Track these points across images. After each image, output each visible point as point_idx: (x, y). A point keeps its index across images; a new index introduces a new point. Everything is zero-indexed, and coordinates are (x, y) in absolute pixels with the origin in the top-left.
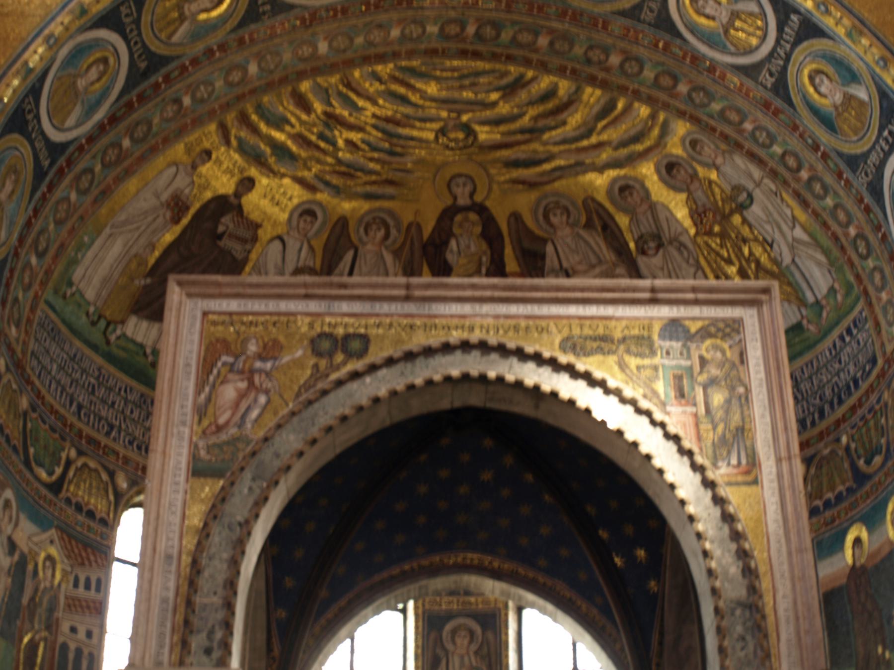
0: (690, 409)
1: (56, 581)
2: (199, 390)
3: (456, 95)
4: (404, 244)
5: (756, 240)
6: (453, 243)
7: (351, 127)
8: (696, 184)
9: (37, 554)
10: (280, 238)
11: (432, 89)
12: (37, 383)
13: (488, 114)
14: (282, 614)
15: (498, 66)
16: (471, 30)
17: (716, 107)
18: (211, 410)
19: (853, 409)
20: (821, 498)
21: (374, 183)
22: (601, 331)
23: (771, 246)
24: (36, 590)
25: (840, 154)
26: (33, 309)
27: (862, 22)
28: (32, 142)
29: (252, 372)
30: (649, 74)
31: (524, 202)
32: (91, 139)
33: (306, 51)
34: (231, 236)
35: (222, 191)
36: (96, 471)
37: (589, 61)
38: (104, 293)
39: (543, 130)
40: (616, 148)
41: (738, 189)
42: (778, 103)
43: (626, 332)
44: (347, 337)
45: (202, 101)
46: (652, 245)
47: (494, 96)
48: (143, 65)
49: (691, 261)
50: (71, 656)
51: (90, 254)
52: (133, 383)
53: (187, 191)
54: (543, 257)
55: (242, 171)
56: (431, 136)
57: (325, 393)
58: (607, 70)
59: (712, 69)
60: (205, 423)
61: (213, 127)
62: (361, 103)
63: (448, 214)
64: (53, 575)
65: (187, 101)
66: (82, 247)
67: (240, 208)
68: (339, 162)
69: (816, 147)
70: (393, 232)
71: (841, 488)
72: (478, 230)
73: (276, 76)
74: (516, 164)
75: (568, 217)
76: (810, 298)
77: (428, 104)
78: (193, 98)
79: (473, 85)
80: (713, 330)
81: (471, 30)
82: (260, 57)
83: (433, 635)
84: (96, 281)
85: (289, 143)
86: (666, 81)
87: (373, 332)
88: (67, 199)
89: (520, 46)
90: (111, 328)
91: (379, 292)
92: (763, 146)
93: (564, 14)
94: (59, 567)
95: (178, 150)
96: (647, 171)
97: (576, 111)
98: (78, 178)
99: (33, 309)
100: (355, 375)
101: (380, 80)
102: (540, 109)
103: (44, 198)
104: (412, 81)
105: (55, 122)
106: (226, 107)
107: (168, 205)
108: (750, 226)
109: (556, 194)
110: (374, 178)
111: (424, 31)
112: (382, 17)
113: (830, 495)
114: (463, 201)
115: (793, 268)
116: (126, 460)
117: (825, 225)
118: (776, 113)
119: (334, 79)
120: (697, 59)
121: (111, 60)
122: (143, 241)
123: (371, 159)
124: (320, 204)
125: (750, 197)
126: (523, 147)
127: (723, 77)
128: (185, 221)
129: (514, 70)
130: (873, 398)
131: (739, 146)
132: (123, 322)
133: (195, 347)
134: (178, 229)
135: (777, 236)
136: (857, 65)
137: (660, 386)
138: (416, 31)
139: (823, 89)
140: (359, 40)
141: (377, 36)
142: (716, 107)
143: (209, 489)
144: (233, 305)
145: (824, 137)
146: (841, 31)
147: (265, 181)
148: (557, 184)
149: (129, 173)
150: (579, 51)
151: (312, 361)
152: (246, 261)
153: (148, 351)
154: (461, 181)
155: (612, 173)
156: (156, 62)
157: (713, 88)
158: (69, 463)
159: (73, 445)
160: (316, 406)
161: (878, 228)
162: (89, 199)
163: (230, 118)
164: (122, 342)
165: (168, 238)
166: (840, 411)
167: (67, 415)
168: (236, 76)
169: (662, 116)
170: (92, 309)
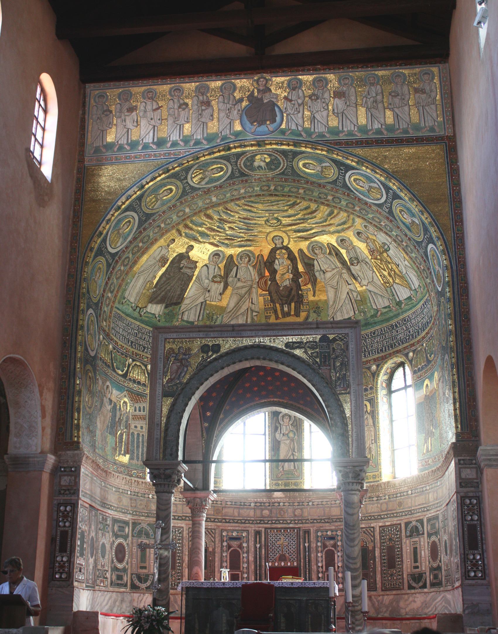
0: (328, 368)
1: (128, 411)
2: (164, 367)
3: (271, 208)
4: (256, 263)
5: (393, 263)
6: (277, 261)
7: (230, 222)
8: (368, 241)
9: (120, 402)
10: (206, 265)
11: (260, 206)
12: (115, 338)
13: (285, 214)
14: (206, 425)
15: (285, 199)
16: (272, 188)
17: (370, 216)
18: (169, 374)
19: (427, 333)
20: (417, 367)
21: (242, 241)
22: (299, 340)
23: (398, 266)
24: (121, 415)
25: (414, 240)
26: (111, 313)
27: (414, 195)
28: (105, 257)
29: (182, 359)
30: (344, 203)
31: (304, 245)
32: (127, 247)
33: (208, 201)
34: (186, 267)
35: (181, 252)
36: (140, 366)
37: (320, 198)
38: (138, 298)
39: (308, 219)
40: (337, 226)
41: (384, 244)
42: (391, 218)
43: (308, 340)
44: (213, 345)
45: (169, 224)
46: (355, 262)
47: (286, 208)
48: (144, 219)
49: (371, 269)
50: (136, 437)
51: (131, 285)
53: (166, 254)
54: (313, 266)
55: (188, 243)
56: (264, 223)
57: (205, 366)
58: (328, 201)
59: (366, 203)
60: (167, 378)
61: (174, 231)
62: (232, 214)
63: (273, 251)
64: (127, 408)
65: (163, 225)
66: (127, 284)
67: (189, 257)
68: (227, 235)
69: (406, 235)
70: (252, 258)
71: (423, 364)
72: (286, 256)
73: (197, 211)
74: (299, 231)
75: (322, 251)
76: (413, 288)
77: (260, 212)
78: (165, 224)
79: (278, 204)
80: (337, 338)
81: (272, 188)
82: (189, 206)
83: (275, 418)
84: (134, 295)
85: (206, 231)
86: (351, 206)
87: (221, 342)
88: (120, 270)
89: (293, 192)
90: (142, 310)
91: (224, 329)
92: (390, 231)
93: (307, 182)
94: (128, 405)
95: (162, 242)
96: (350, 235)
97: (319, 213)
98: (124, 261)
99: (111, 313)
100: (215, 359)
101: (239, 206)
102: (305, 212)
103: (111, 273)
104: (253, 205)
105: (113, 246)
106: (179, 224)
107: (159, 260)
108: (390, 258)
109: (316, 242)
110: (242, 239)
111: (254, 189)
112: (235, 187)
113: (420, 366)
114: (278, 246)
115: (406, 275)
117: (414, 262)
118: (391, 221)
119: (221, 208)
120: (359, 199)
121: (132, 220)
122: (151, 276)
123: (240, 233)
124: (221, 251)
125: (388, 246)
126: (301, 225)
127: (370, 206)
128: (167, 266)
129: (292, 200)
130: (432, 331)
131: (381, 229)
132: (146, 307)
133: (163, 351)
134: (164, 269)
135: (400, 263)
136: (414, 211)
137: (318, 360)
138: (250, 190)
139: (405, 216)
140: (228, 195)
141: (235, 193)
142: (370, 216)
143: (169, 401)
144: (175, 335)
145: (408, 233)
146: (407, 198)
147: (197, 245)
148: (316, 238)
149: (143, 254)
150: (316, 194)
152: (193, 275)
153: (157, 316)
154: (277, 238)
155: (337, 234)
156: (148, 216)
157: (368, 210)
158: (129, 365)
159: (130, 358)
160: (203, 371)
161: (429, 269)
162: (128, 267)
163: (181, 227)
164: (146, 315)
165: (160, 273)
166: (424, 333)
167: (127, 347)
168: (181, 214)
169: (352, 216)
170: (133, 305)
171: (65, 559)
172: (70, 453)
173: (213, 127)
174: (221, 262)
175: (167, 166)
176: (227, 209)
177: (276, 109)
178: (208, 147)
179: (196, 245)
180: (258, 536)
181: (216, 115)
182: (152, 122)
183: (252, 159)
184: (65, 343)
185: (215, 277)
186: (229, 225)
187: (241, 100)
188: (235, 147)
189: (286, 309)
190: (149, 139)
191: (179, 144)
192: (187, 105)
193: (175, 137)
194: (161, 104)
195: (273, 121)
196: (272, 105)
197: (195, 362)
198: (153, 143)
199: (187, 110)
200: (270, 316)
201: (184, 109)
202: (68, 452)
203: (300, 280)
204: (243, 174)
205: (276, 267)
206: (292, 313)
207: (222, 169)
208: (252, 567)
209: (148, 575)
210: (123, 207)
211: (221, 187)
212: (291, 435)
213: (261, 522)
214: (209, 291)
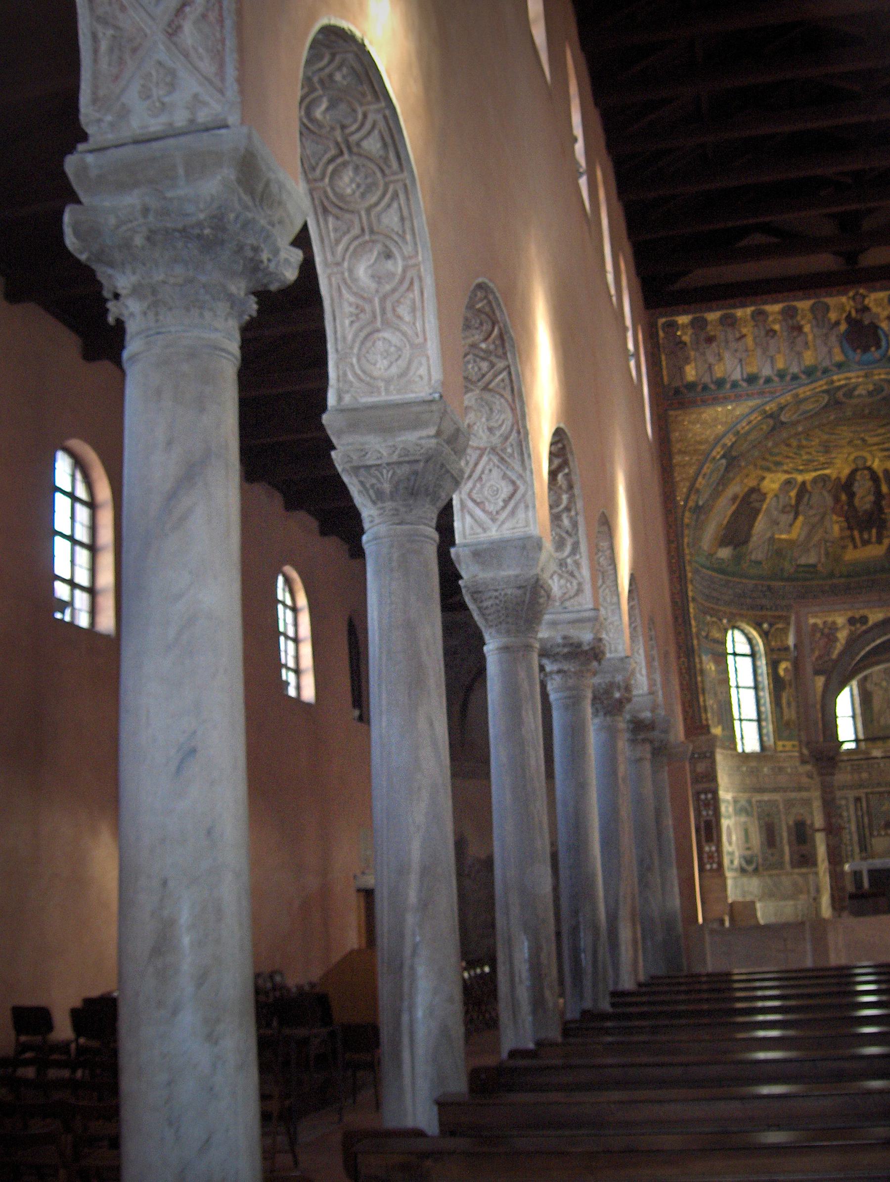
6: (856, 484)
10: (776, 496)
11: (845, 428)
36: (716, 623)
52: (721, 576)
61: (751, 467)
72: (868, 477)
81: (867, 411)
100: (866, 632)
114: (860, 466)
116: (725, 613)
124: (792, 478)
132: (715, 553)
134: (734, 507)
144: (817, 609)
151: (847, 626)
156: (734, 458)
171: (714, 848)
172: (703, 738)
173: (809, 358)
174: (793, 489)
175: (762, 408)
176: (808, 435)
177: (880, 333)
178: (806, 382)
179: (769, 476)
180: (859, 805)
181: (810, 344)
182: (738, 355)
183: (855, 388)
184: (677, 618)
185: (785, 507)
186: (807, 450)
187: (837, 323)
188: (839, 380)
189: (866, 536)
190: (737, 375)
191: (772, 380)
192: (774, 332)
193: (767, 371)
194: (744, 331)
195: (878, 347)
196: (874, 328)
197: (842, 636)
198: (743, 380)
199: (776, 338)
200: (848, 546)
201: (772, 337)
202: (700, 738)
203: (884, 503)
204: (838, 403)
205: (855, 489)
206: (874, 539)
207: (817, 401)
208: (855, 838)
209: (752, 857)
210: (718, 457)
211: (812, 416)
212: (884, 684)
213: (861, 786)
214: (778, 524)
